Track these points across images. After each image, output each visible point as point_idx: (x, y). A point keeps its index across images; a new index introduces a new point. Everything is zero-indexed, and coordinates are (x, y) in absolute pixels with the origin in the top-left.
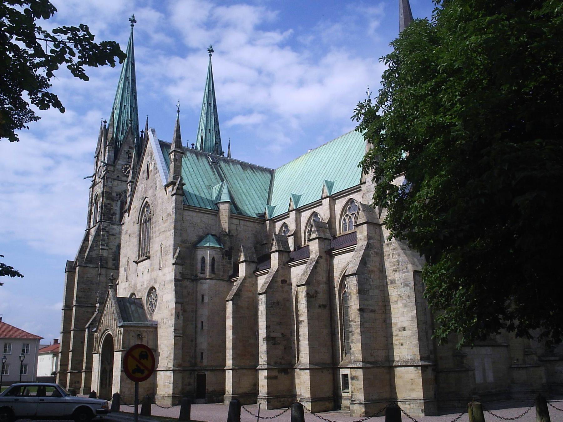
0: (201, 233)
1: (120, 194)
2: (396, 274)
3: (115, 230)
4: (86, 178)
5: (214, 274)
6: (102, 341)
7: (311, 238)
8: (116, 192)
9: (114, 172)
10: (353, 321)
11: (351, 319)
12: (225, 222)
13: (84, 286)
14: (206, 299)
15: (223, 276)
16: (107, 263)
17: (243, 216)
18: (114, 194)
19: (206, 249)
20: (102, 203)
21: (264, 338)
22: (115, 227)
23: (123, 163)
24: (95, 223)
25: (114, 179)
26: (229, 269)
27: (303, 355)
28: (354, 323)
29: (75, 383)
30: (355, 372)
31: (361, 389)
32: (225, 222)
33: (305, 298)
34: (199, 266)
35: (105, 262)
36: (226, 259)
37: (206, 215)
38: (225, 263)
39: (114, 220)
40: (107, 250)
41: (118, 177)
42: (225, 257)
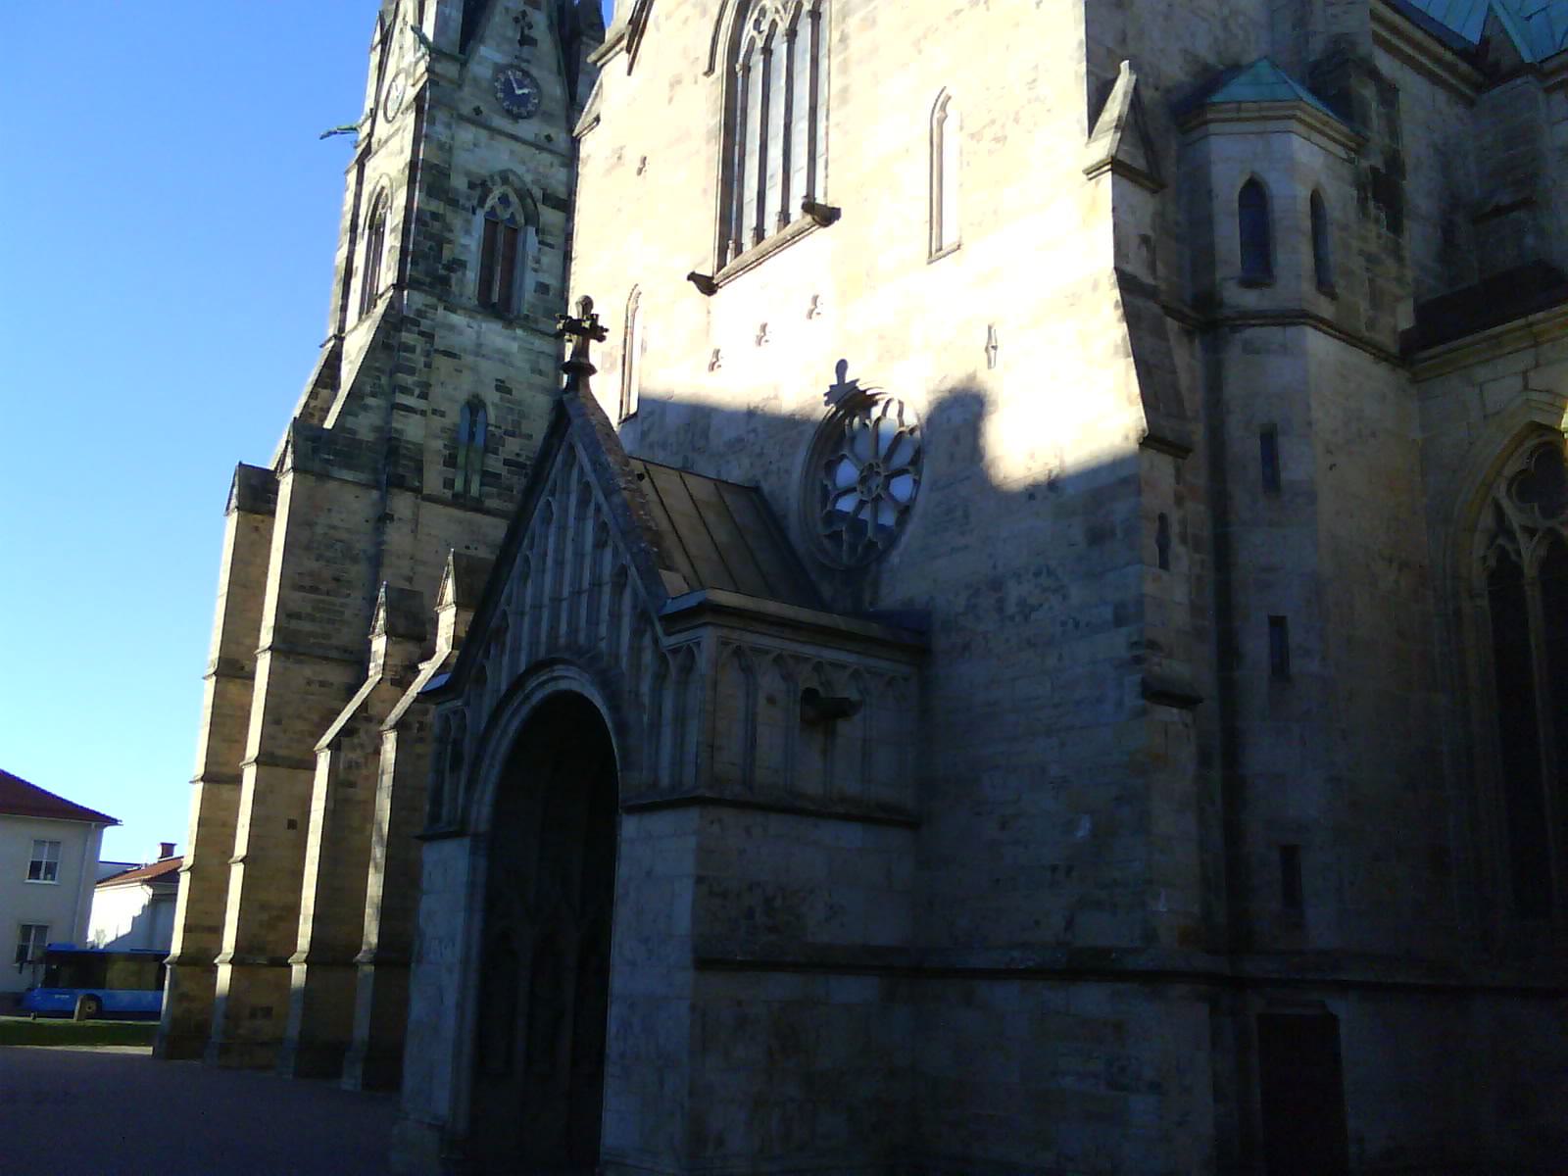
0: (1204, 50)
1: (483, 184)
3: (461, 333)
4: (330, 134)
5: (1333, 296)
6: (502, 744)
8: (468, 174)
9: (460, 86)
13: (315, 565)
15: (1371, 324)
16: (420, 471)
18: (459, 183)
19: (1271, 125)
20: (408, 208)
22: (458, 319)
23: (499, 58)
24: (369, 301)
25: (461, 118)
29: (253, 1015)
34: (1228, 236)
35: (412, 464)
36: (1377, 221)
38: (1373, 247)
39: (455, 289)
40: (423, 413)
41: (477, 111)
42: (1371, 204)
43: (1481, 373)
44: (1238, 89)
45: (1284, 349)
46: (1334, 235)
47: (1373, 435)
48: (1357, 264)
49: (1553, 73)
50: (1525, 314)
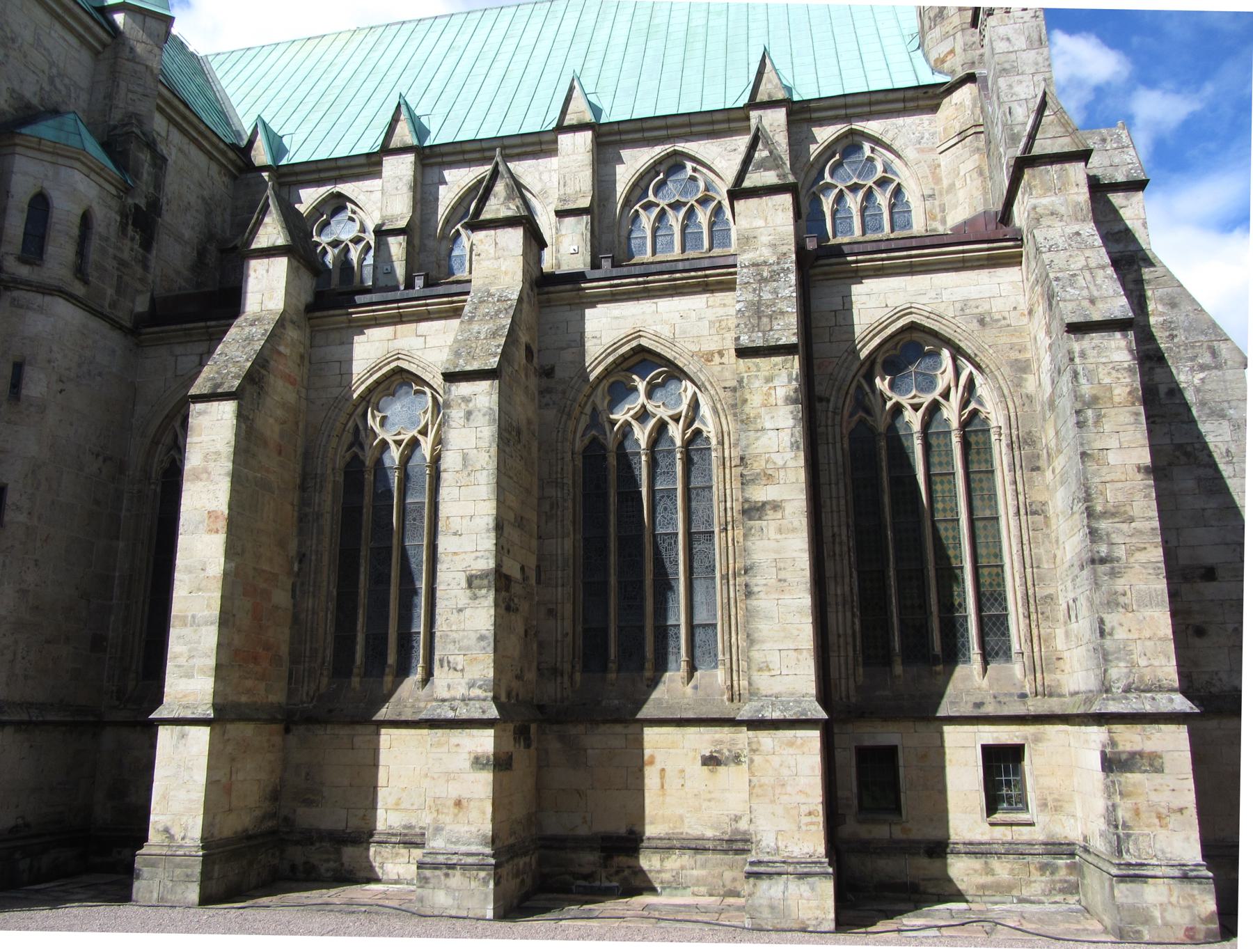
0: (30, 91)
2: (1158, 370)
5: (86, 282)
7: (747, 184)
10: (1113, 515)
11: (1099, 508)
12: (140, 90)
14: (36, 385)
15: (113, 305)
17: (187, 113)
19: (61, 160)
21: (483, 575)
26: (139, 286)
27: (774, 659)
28: (1125, 527)
30: (1138, 738)
31: (1181, 810)
32: (140, 90)
33: (791, 407)
34: (16, 224)
36: (133, 239)
37: (58, 26)
38: (126, 255)
42: (130, 228)
43: (179, 350)
44: (45, 130)
45: (41, 310)
46: (94, 243)
47: (100, 374)
48: (110, 264)
49: (284, 175)
50: (206, 320)
